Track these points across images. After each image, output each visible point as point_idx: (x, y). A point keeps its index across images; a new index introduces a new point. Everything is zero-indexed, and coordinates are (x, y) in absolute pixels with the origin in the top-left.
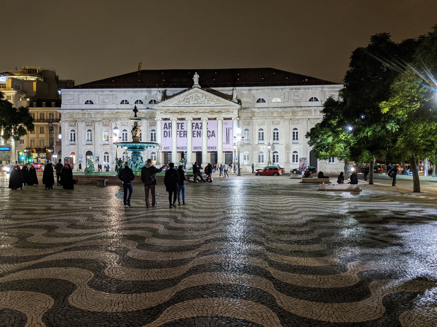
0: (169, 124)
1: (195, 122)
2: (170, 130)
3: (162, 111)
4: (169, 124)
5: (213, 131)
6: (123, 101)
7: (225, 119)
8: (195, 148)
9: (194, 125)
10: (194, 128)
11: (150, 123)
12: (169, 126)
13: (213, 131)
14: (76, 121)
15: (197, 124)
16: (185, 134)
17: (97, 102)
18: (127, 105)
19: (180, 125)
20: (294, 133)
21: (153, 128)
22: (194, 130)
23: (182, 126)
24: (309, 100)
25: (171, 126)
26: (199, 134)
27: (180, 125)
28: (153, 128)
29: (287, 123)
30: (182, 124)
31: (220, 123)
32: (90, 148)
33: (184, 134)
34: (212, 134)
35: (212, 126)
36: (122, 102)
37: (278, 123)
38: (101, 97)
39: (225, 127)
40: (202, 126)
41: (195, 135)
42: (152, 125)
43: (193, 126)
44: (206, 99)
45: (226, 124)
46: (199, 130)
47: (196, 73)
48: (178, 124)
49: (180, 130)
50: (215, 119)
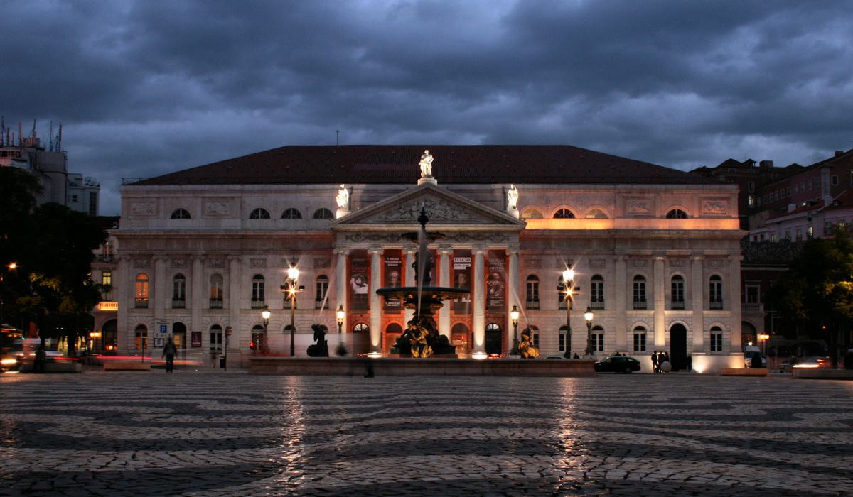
3: (349, 234)
6: (256, 211)
11: (315, 260)
14: (150, 256)
17: (199, 214)
18: (265, 220)
20: (636, 286)
24: (666, 214)
28: (321, 271)
29: (621, 266)
32: (180, 316)
36: (254, 215)
37: (602, 266)
38: (208, 204)
44: (448, 208)
47: (427, 152)
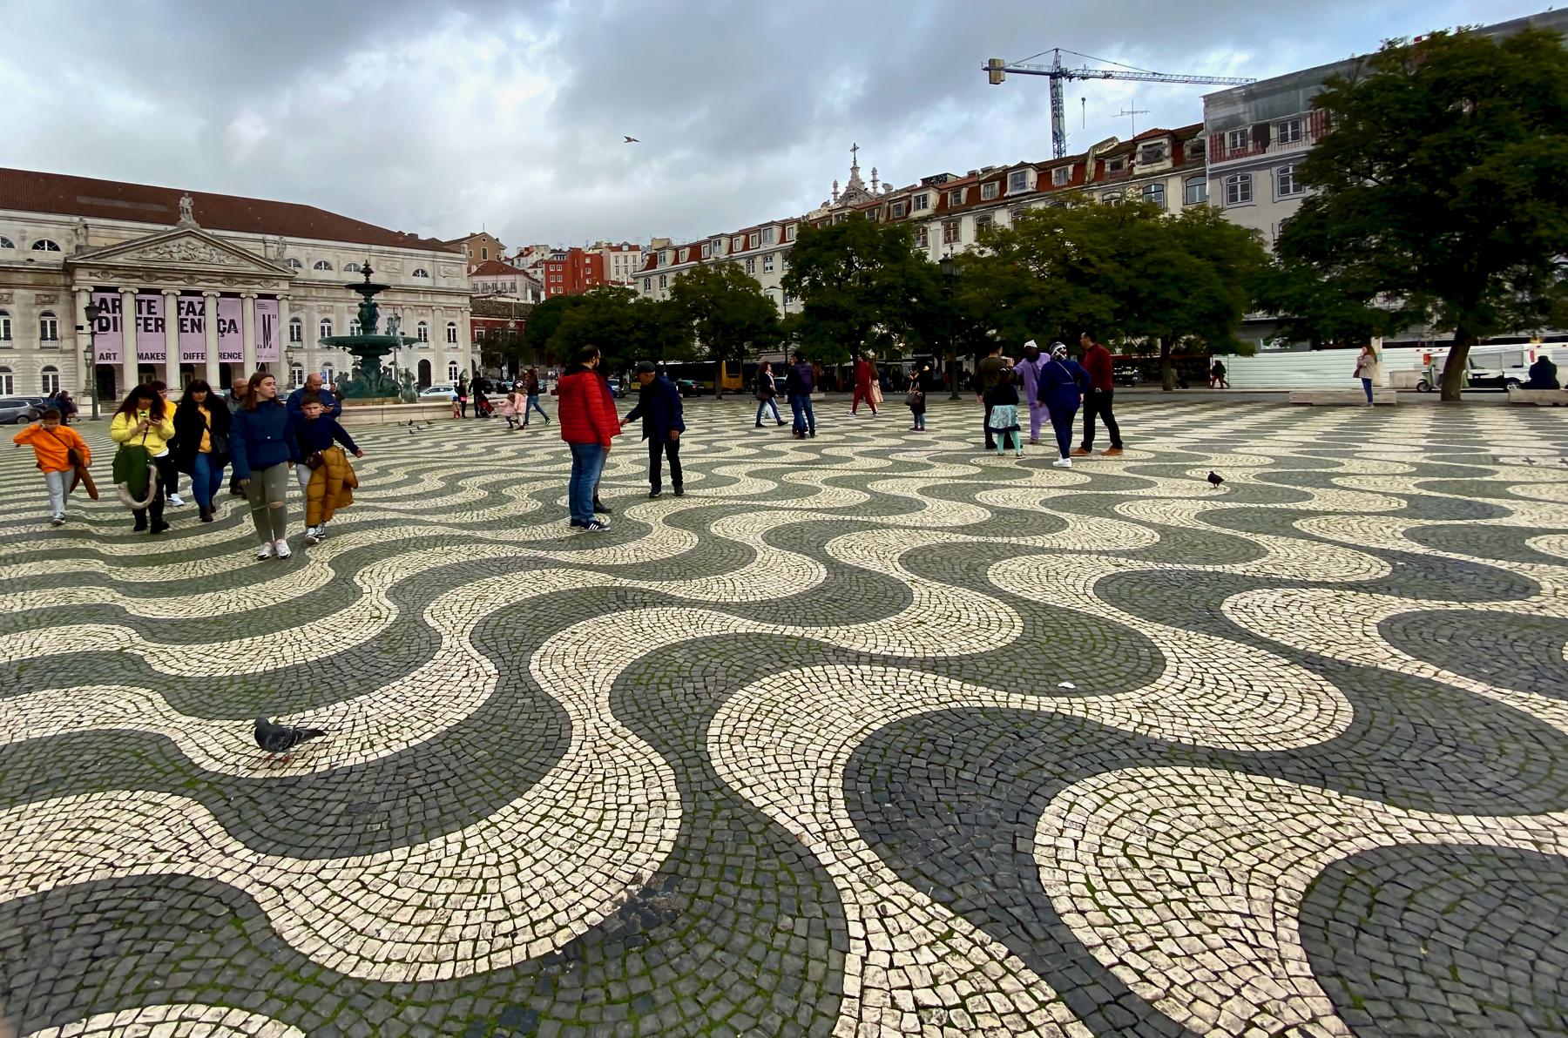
0: (114, 300)
1: (188, 299)
2: (118, 315)
4: (114, 300)
5: (232, 322)
7: (261, 296)
8: (186, 356)
9: (185, 306)
10: (183, 312)
12: (114, 307)
13: (232, 322)
15: (191, 304)
16: (161, 325)
19: (144, 305)
21: (47, 308)
22: (183, 316)
23: (150, 307)
25: (120, 307)
26: (198, 326)
27: (144, 305)
28: (47, 308)
30: (149, 302)
31: (249, 304)
33: (157, 326)
34: (228, 327)
35: (230, 310)
39: (260, 313)
40: (203, 309)
41: (188, 328)
42: (44, 303)
43: (179, 309)
45: (262, 307)
46: (196, 318)
48: (140, 302)
49: (145, 314)
50: (236, 295)
